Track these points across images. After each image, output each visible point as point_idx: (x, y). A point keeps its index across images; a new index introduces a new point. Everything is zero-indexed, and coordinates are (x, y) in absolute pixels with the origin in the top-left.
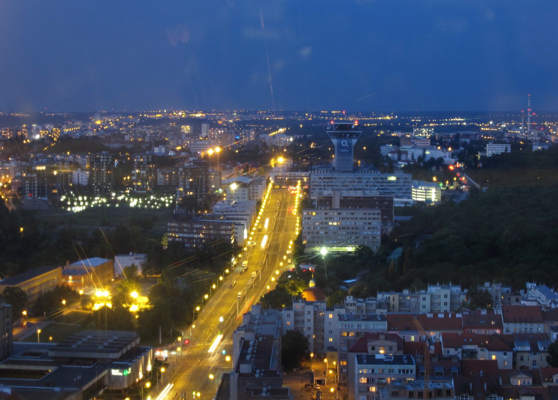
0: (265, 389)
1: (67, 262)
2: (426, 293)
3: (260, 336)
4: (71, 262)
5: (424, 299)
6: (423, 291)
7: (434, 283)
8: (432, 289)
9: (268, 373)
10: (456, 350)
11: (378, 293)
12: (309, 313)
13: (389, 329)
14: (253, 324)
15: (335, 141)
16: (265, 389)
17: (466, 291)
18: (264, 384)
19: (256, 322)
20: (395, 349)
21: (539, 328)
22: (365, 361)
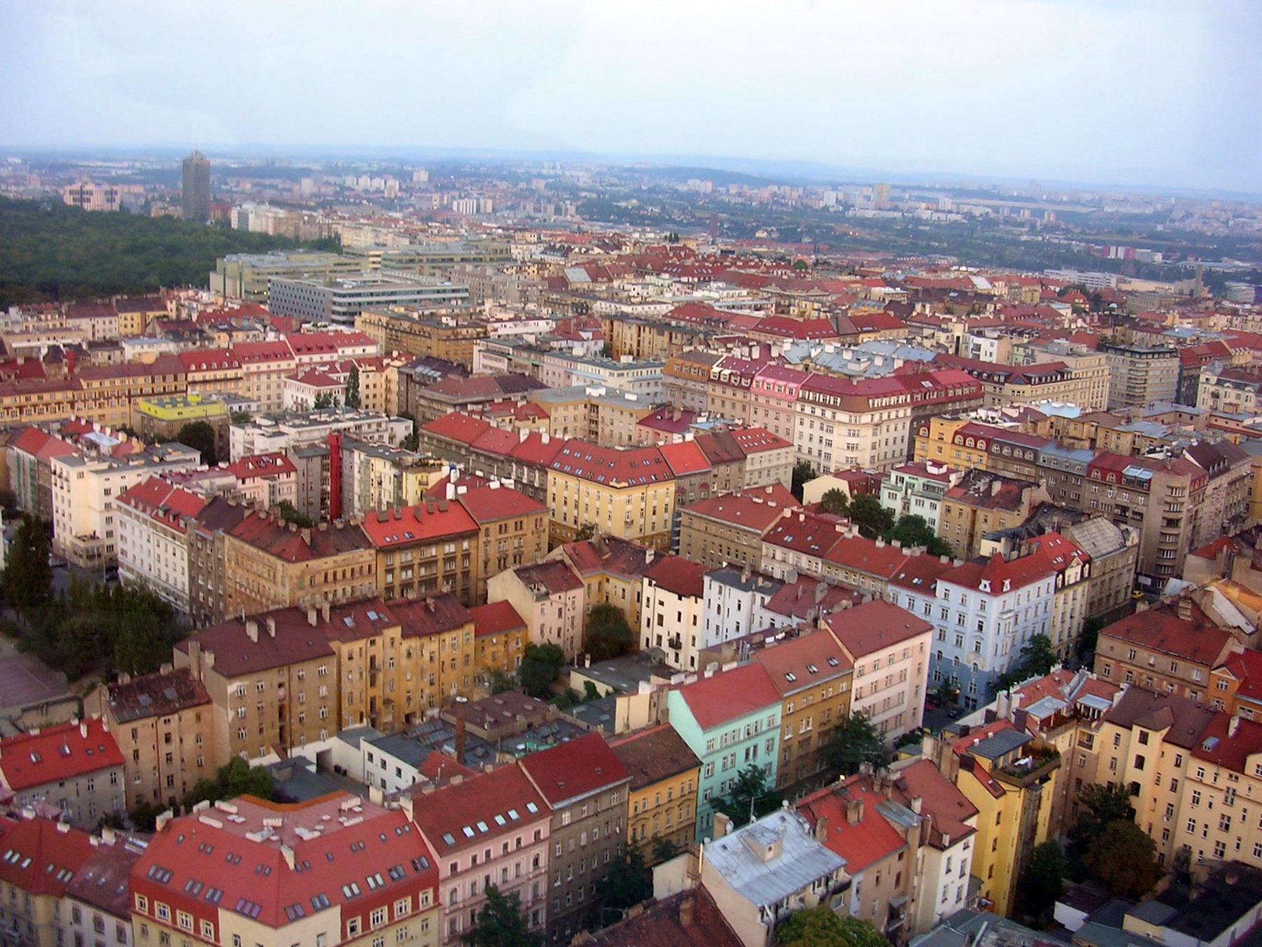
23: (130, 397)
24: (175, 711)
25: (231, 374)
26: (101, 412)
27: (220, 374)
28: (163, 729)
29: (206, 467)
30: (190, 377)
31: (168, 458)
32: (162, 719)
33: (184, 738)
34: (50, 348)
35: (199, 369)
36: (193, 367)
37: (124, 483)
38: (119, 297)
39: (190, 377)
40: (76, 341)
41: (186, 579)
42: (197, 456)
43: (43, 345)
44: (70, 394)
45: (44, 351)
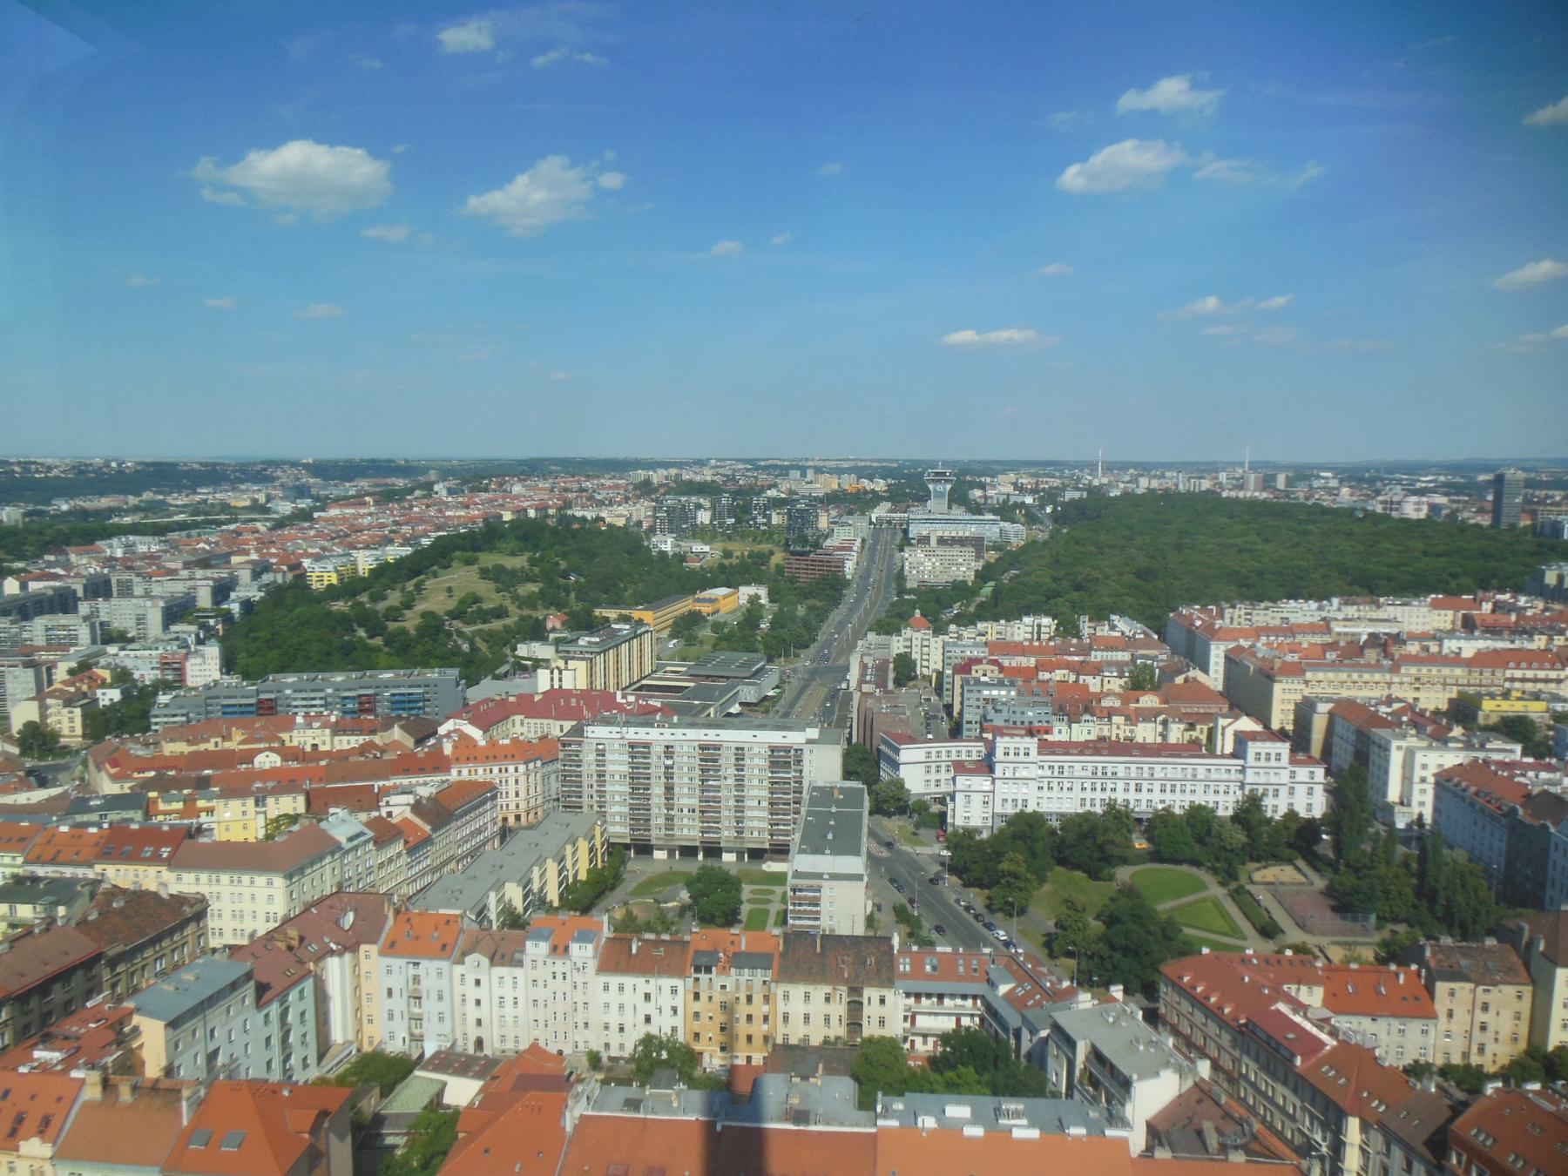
7: (1027, 614)
8: (1027, 620)
9: (887, 692)
13: (991, 654)
15: (931, 487)
21: (1123, 656)
23: (1445, 685)
24: (1495, 985)
25: (1553, 675)
26: (1416, 695)
27: (1541, 674)
28: (1481, 996)
29: (1530, 760)
30: (1509, 673)
31: (1488, 746)
32: (1481, 988)
33: (1502, 1011)
34: (1371, 635)
35: (1517, 668)
36: (1512, 664)
37: (1441, 761)
38: (1433, 596)
39: (1509, 673)
40: (1394, 630)
41: (1502, 861)
42: (1518, 748)
43: (1364, 631)
44: (1388, 676)
45: (1364, 638)
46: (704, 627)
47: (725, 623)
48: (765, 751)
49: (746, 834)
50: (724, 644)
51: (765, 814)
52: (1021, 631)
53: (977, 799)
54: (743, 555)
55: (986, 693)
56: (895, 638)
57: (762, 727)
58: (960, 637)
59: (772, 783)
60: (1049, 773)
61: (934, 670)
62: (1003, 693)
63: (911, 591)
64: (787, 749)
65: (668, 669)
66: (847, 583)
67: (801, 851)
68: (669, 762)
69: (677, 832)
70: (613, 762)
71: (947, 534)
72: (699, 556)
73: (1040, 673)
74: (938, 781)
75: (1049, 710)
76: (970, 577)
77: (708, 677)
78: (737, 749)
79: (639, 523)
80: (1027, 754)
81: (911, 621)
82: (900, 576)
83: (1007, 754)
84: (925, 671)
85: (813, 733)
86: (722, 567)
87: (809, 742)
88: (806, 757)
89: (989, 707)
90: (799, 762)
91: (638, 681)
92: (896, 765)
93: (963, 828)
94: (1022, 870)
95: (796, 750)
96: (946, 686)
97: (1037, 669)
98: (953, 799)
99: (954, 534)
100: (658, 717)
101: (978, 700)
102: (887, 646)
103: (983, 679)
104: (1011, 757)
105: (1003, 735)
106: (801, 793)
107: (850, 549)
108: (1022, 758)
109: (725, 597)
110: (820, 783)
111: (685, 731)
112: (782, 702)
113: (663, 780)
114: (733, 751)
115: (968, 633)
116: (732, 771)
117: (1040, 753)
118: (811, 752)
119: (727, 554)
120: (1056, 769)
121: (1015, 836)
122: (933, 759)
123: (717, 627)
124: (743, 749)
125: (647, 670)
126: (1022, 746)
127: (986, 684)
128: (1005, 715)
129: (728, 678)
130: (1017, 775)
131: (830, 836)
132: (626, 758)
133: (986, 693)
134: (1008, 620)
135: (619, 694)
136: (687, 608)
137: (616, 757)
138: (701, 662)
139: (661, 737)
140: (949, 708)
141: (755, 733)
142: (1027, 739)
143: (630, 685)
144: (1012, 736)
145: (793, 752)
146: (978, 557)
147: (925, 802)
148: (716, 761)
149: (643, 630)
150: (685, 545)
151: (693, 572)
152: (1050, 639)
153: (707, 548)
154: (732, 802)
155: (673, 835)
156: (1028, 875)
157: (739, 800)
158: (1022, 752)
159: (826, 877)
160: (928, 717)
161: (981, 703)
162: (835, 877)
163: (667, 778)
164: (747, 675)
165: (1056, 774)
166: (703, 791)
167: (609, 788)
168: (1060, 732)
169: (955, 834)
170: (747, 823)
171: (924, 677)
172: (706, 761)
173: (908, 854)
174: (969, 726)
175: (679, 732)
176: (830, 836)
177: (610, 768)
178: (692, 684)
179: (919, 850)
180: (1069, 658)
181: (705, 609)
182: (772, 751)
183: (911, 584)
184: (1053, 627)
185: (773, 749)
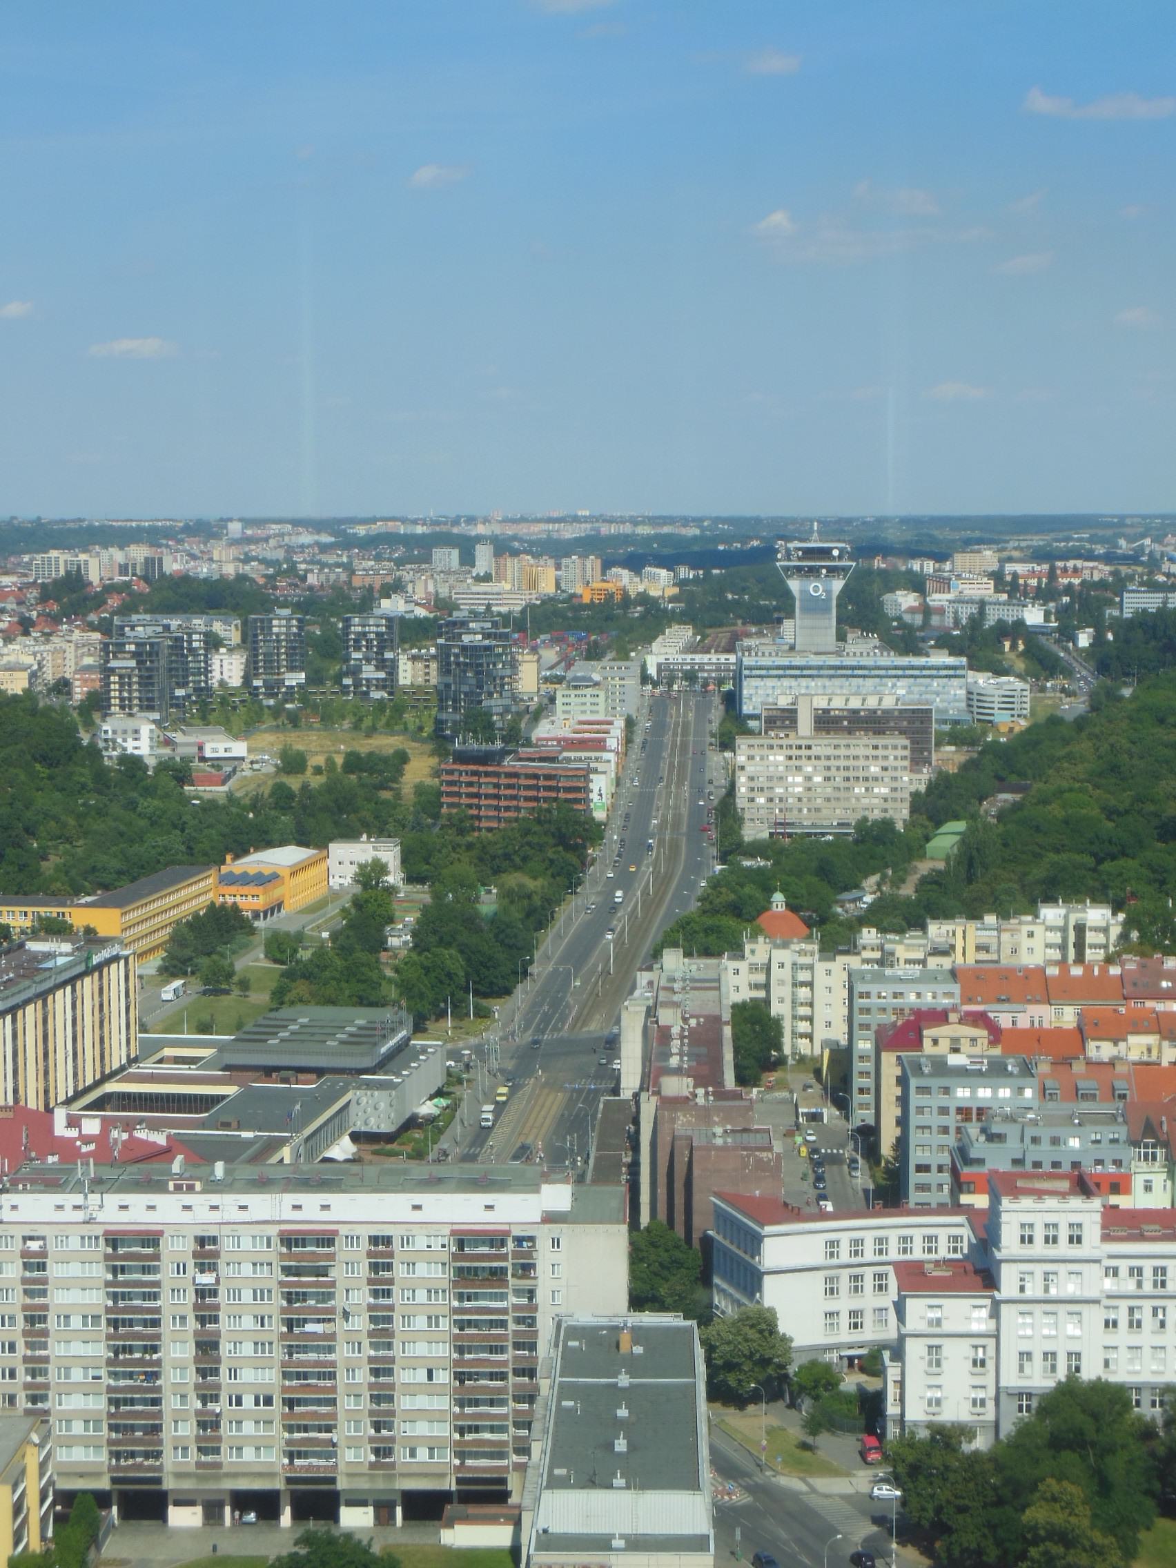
0: (719, 1130)
1: (229, 858)
2: (1033, 923)
3: (692, 1016)
4: (237, 857)
5: (1031, 935)
6: (1029, 918)
7: (1050, 899)
8: (1052, 914)
9: (721, 1095)
10: (1116, 1044)
11: (929, 921)
12: (782, 965)
14: (672, 990)
15: (794, 585)
16: (719, 1130)
17: (1121, 916)
18: (716, 1119)
19: (677, 986)
20: (983, 1042)
22: (926, 1070)
46: (245, 947)
47: (299, 937)
48: (441, 1243)
49: (401, 1456)
50: (301, 988)
51: (443, 1403)
52: (1038, 942)
53: (957, 1354)
54: (330, 762)
55: (962, 1093)
56: (727, 963)
57: (433, 1184)
58: (886, 960)
59: (461, 1325)
60: (1130, 1286)
61: (826, 1043)
62: (1004, 1093)
63: (756, 849)
64: (496, 1239)
65: (168, 1052)
66: (594, 832)
67: (555, 1483)
68: (207, 1279)
69: (227, 1457)
70: (67, 1284)
71: (838, 703)
72: (223, 768)
73: (1091, 1046)
74: (854, 1314)
75: (1121, 1132)
76: (901, 814)
77: (268, 1071)
78: (374, 1240)
79: (63, 687)
80: (1076, 1240)
81: (763, 920)
82: (727, 811)
83: (1027, 1240)
84: (804, 1046)
85: (558, 1196)
86: (282, 797)
87: (550, 1218)
88: (544, 1257)
89: (973, 1129)
90: (526, 1269)
91: (97, 1084)
92: (751, 1280)
93: (930, 1426)
94: (1081, 1521)
95: (519, 1240)
96: (858, 1082)
97: (1081, 1034)
98: (898, 1353)
99: (855, 703)
100: (176, 1167)
101: (944, 1111)
102: (715, 984)
103: (954, 1060)
104: (1039, 1248)
105: (1016, 1193)
106: (532, 1347)
107: (599, 745)
108: (1063, 1248)
109: (296, 870)
110: (584, 1317)
111: (244, 1199)
112: (457, 1129)
113: (192, 1324)
114: (365, 1246)
115: (907, 948)
116: (362, 1297)
117: (1106, 1238)
118: (556, 1243)
119: (293, 763)
120: (1148, 1273)
121: (1057, 1443)
122: (845, 1257)
123: (280, 946)
124: (387, 1240)
125: (117, 1057)
126: (1063, 1221)
127: (962, 1072)
128: (1013, 1147)
129: (320, 1072)
130: (1053, 1292)
131: (621, 1445)
132: (100, 1272)
133: (962, 1093)
134: (1004, 915)
135: (60, 1116)
136: (204, 901)
137: (74, 1269)
138: (254, 1037)
139: (187, 1217)
140: (868, 1136)
141: (417, 1198)
142: (1076, 1202)
143: (78, 1095)
144: (1039, 1194)
145: (511, 1245)
146: (918, 759)
147: (828, 1367)
148: (323, 1272)
149: (106, 954)
150: (185, 740)
151: (210, 806)
152: (1109, 960)
153: (239, 748)
154: (363, 1376)
155: (218, 1465)
156: (1098, 1538)
157: (381, 1369)
158: (1063, 1235)
159: (618, 1543)
160: (819, 1162)
161: (952, 1120)
162: (637, 1543)
163: (202, 1320)
164: (367, 1062)
165: (1148, 1287)
166: (290, 1351)
167: (56, 1349)
168: (1148, 1188)
169: (907, 1441)
170: (402, 1429)
171: (802, 1060)
172: (297, 1272)
173: (795, 1496)
174: (923, 1177)
175: (229, 1202)
176: (621, 1445)
177: (58, 1298)
178: (230, 1090)
179: (824, 1484)
180: (1160, 1007)
181: (249, 901)
182: (461, 1244)
183: (753, 832)
184: (1115, 931)
185: (462, 1239)
